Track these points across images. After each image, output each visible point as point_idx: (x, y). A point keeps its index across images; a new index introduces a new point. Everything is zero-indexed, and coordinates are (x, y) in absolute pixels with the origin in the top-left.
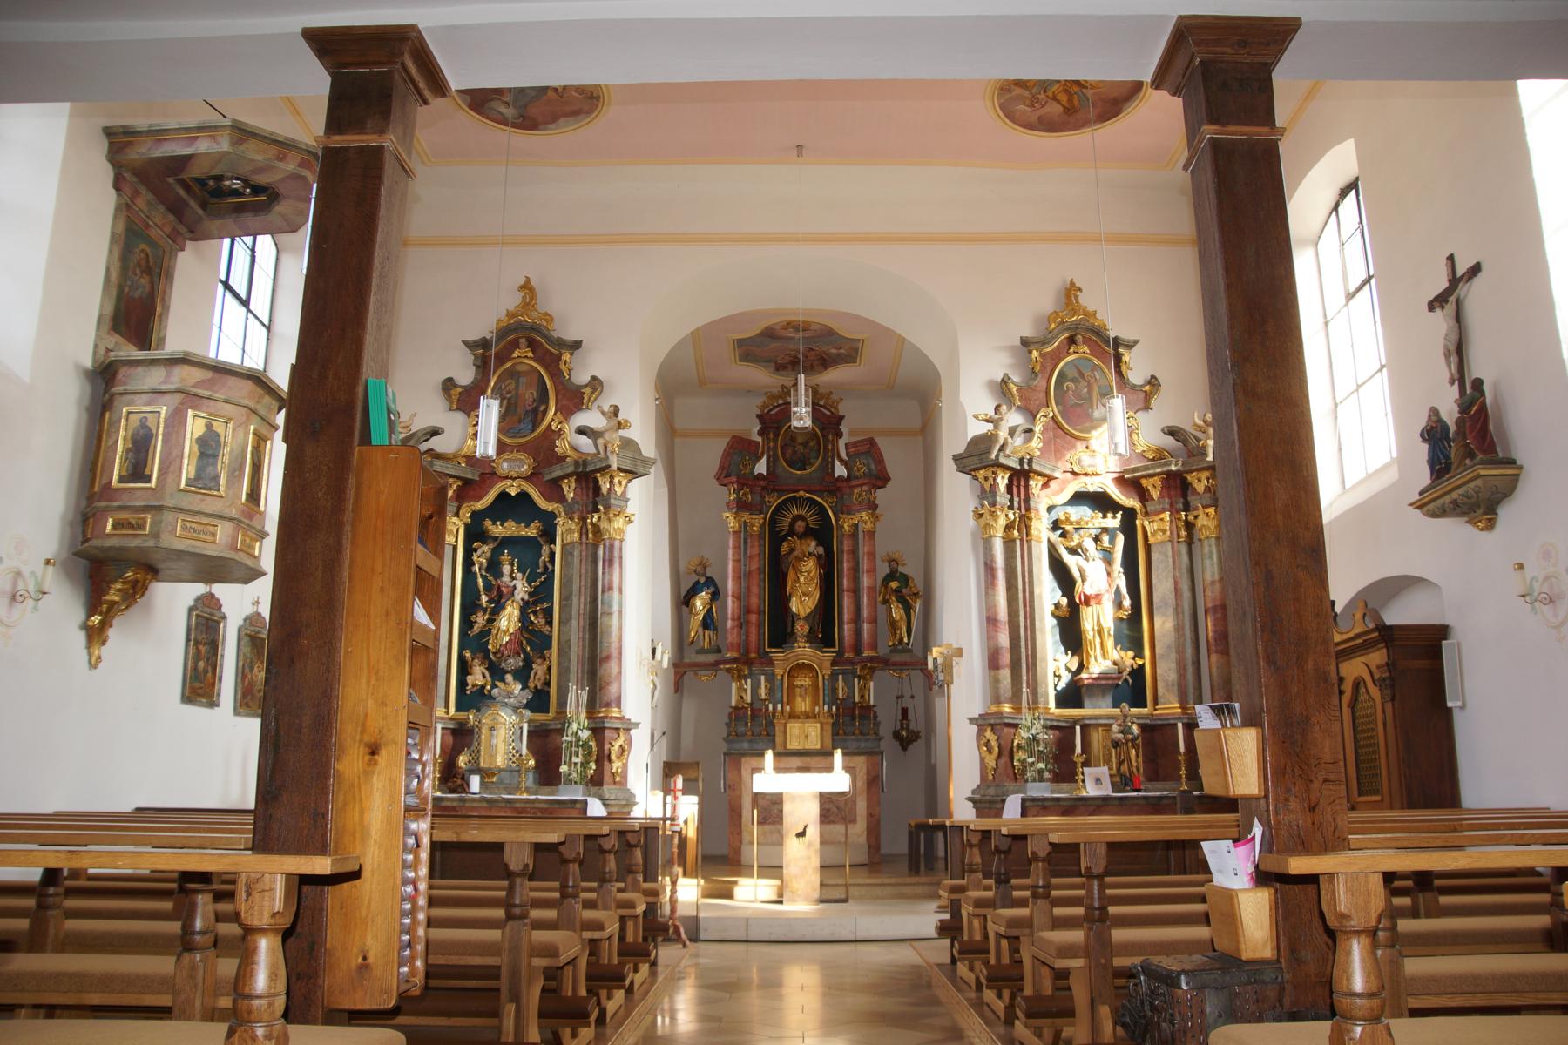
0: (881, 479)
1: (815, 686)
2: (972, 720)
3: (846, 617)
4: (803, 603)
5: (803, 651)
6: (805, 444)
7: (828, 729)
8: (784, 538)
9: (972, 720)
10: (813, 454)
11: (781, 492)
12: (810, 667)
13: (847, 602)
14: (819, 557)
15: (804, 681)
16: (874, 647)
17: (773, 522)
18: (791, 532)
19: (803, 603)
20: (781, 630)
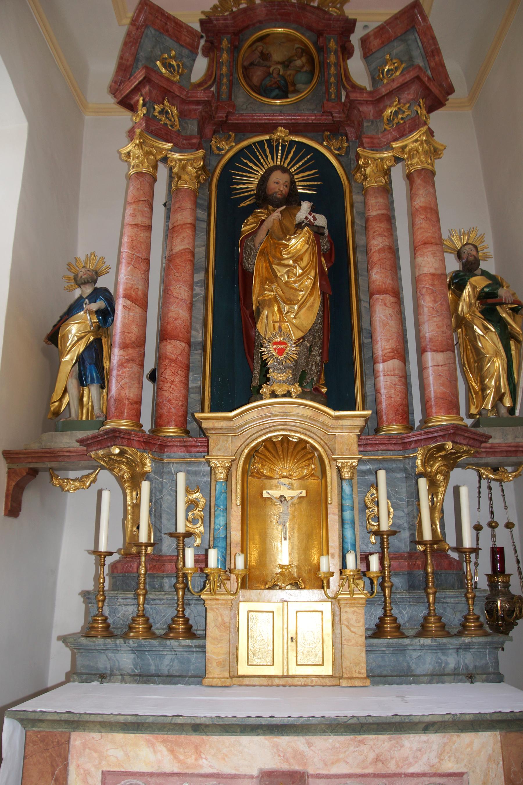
0: (435, 94)
1: (316, 503)
2: (481, 549)
3: (383, 344)
4: (287, 317)
5: (281, 411)
6: (287, 64)
7: (357, 621)
8: (249, 211)
9: (481, 549)
10: (302, 77)
11: (243, 129)
12: (301, 451)
13: (382, 314)
14: (318, 232)
15: (284, 488)
16: (452, 406)
17: (227, 180)
18: (263, 198)
19: (287, 317)
20: (236, 377)
